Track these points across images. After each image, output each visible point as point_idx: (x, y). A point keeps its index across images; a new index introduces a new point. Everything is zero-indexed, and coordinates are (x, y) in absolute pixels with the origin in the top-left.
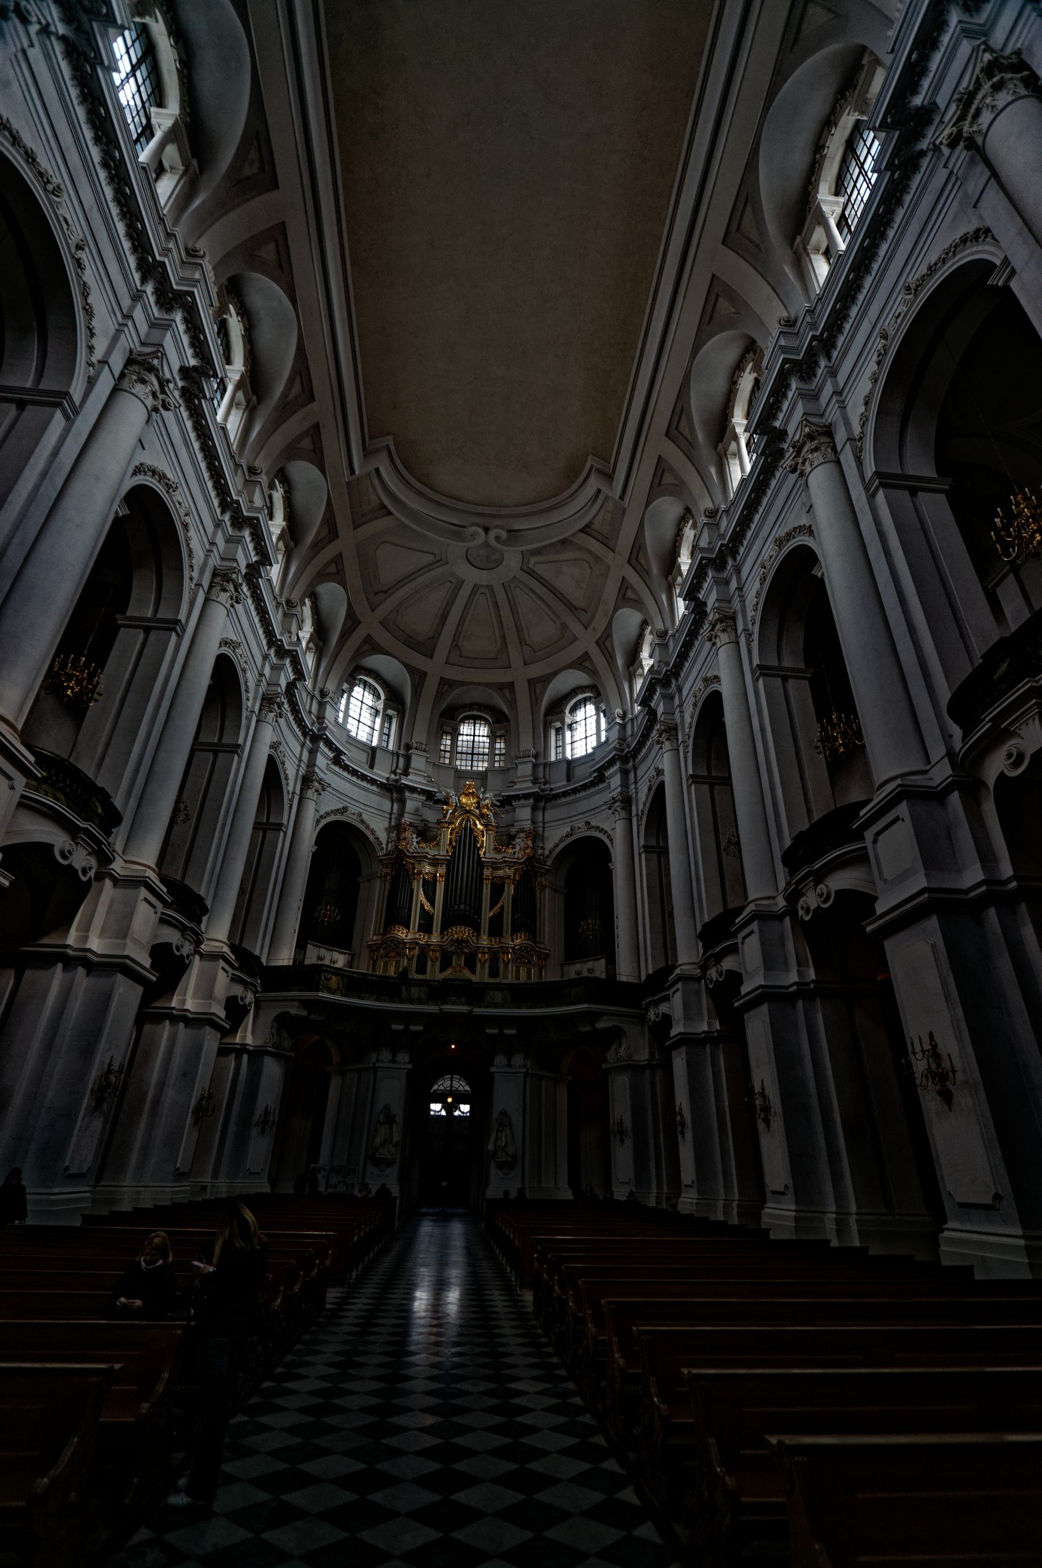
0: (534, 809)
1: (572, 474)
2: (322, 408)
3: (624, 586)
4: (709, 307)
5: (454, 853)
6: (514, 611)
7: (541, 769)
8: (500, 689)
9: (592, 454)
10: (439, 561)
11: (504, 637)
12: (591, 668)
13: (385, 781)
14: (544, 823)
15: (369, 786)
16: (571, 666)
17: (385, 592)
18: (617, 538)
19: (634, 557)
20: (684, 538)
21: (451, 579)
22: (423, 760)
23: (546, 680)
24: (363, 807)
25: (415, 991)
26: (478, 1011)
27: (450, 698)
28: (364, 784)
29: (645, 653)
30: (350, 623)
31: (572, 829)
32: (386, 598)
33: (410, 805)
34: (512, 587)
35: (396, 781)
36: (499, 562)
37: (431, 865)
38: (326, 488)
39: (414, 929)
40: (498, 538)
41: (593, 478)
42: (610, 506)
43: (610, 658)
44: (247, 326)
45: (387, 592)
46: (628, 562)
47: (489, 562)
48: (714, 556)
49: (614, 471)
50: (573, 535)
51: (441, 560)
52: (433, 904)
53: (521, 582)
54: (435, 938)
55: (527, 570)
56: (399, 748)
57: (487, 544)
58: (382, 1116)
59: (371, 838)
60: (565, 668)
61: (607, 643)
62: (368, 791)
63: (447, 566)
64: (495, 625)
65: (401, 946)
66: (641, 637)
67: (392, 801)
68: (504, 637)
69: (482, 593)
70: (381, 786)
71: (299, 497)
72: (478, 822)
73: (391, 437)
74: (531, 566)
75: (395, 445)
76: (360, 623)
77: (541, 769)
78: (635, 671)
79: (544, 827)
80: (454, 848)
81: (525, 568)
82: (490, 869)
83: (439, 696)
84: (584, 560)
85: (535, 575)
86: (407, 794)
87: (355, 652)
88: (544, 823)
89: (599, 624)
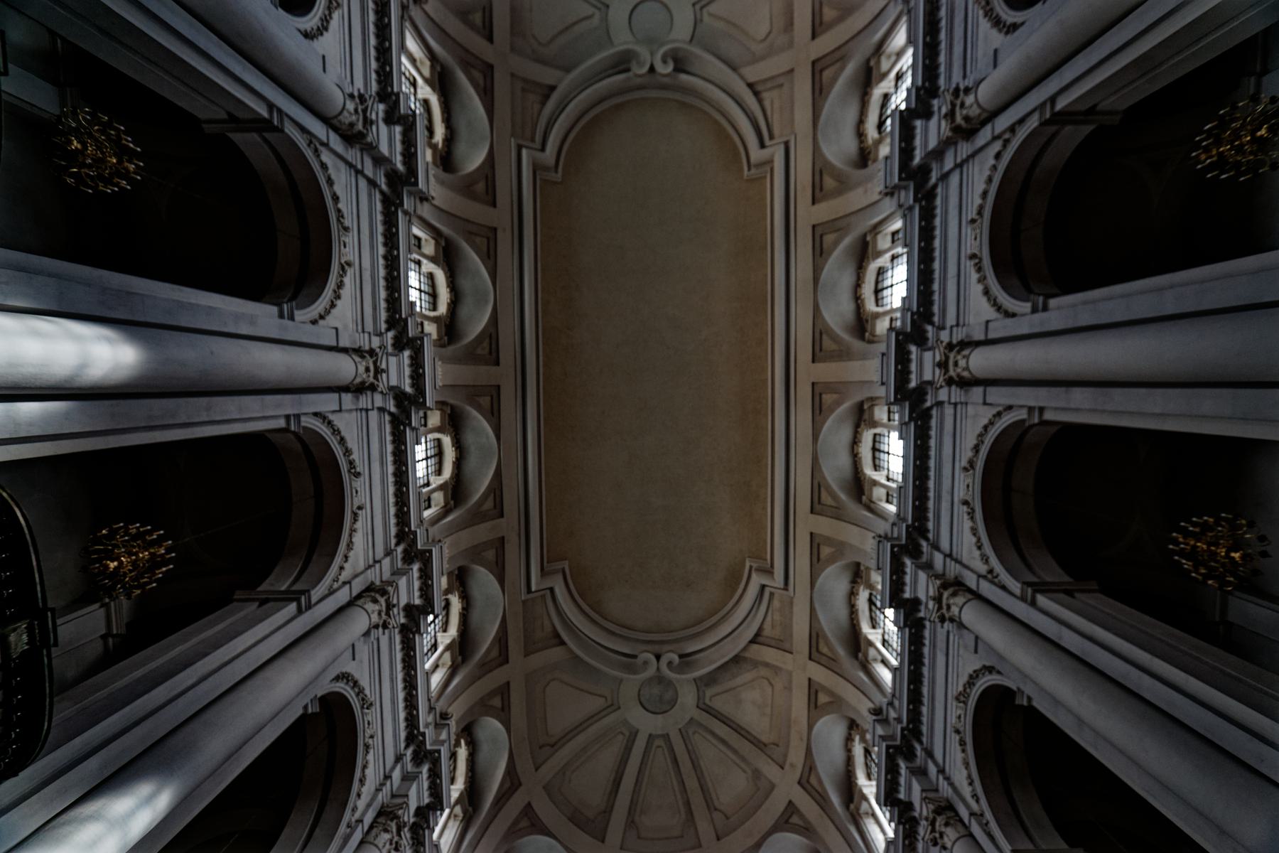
1: (734, 581)
2: (508, 525)
3: (813, 689)
4: (817, 245)
9: (749, 557)
10: (613, 707)
12: (801, 823)
16: (775, 829)
17: (552, 746)
18: (791, 636)
19: (814, 650)
20: (860, 613)
29: (862, 780)
30: (507, 785)
32: (554, 753)
34: (690, 733)
36: (673, 703)
38: (502, 604)
40: (670, 664)
41: (754, 576)
42: (776, 603)
43: (821, 800)
44: (458, 456)
45: (555, 746)
46: (810, 658)
47: (662, 703)
48: (898, 742)
49: (772, 566)
50: (745, 649)
51: (612, 705)
53: (700, 725)
55: (704, 707)
57: (660, 679)
61: (813, 781)
63: (618, 712)
64: (676, 789)
66: (849, 761)
69: (659, 747)
71: (475, 616)
73: (567, 562)
74: (707, 701)
75: (570, 570)
76: (520, 784)
78: (858, 809)
81: (701, 705)
84: (763, 678)
87: (509, 829)
89: (796, 757)
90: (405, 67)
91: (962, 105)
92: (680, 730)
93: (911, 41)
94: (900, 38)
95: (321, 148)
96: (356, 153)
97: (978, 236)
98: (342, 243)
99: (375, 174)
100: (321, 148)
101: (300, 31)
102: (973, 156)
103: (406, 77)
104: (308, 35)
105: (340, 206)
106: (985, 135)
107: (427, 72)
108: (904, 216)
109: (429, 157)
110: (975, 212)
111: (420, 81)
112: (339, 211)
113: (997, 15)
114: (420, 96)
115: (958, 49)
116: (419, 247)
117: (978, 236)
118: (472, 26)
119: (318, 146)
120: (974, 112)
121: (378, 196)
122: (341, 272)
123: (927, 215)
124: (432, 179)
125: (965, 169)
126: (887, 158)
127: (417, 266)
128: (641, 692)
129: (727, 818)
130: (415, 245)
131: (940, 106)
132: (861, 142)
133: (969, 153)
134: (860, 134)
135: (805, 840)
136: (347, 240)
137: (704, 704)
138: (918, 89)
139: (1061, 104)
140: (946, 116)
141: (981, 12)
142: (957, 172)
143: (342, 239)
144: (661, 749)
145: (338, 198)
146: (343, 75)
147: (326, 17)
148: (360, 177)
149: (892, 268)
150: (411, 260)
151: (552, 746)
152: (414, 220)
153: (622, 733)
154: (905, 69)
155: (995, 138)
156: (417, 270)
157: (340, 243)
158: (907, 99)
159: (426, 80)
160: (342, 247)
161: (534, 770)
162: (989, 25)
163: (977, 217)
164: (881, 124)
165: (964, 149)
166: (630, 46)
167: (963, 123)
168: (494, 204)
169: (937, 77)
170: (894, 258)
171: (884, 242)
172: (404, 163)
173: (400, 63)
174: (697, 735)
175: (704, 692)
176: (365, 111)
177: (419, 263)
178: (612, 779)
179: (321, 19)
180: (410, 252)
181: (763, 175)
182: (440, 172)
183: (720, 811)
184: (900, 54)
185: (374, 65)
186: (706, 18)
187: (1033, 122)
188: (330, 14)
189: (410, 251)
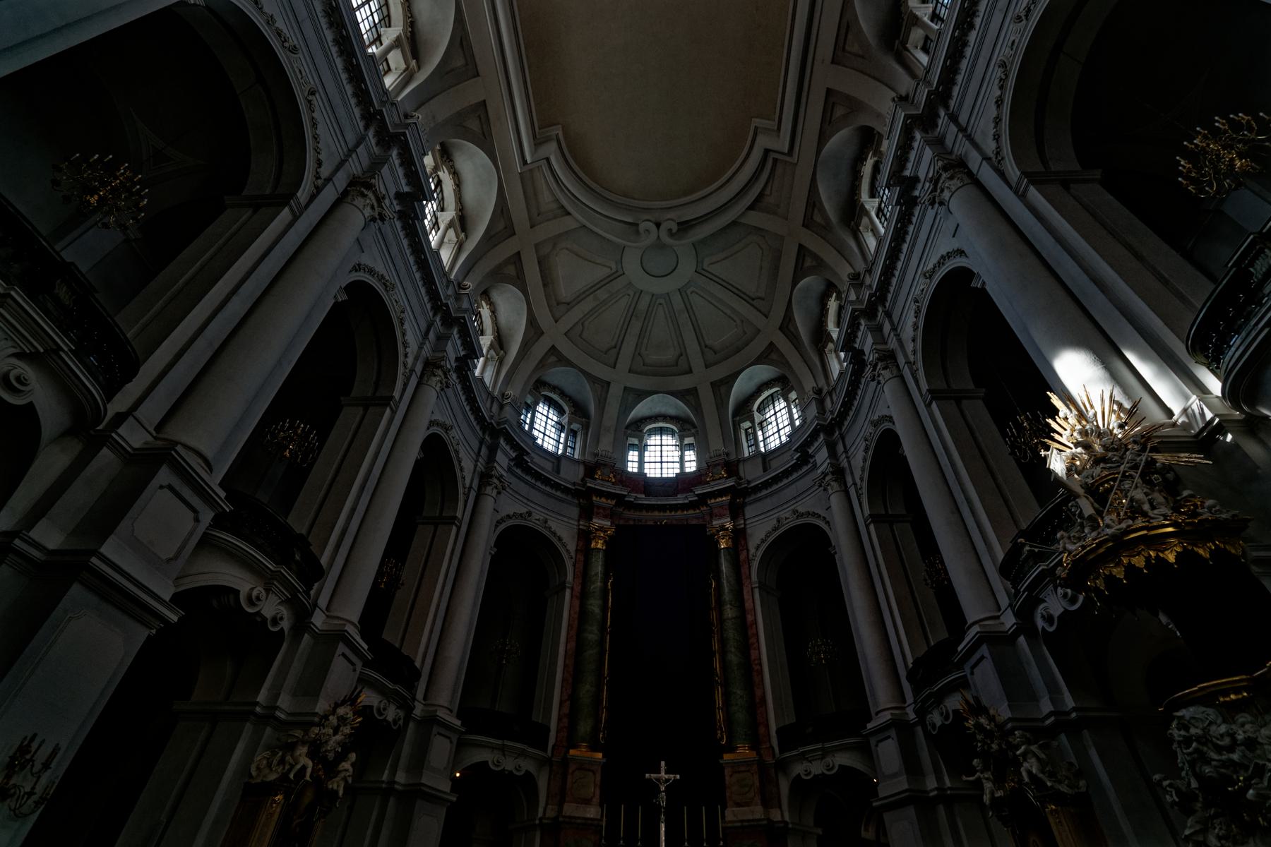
90: (883, 225)
91: (373, 207)
93: (436, 254)
94: (446, 255)
95: (992, 156)
96: (958, 150)
97: (299, 77)
98: (1014, 47)
99: (947, 127)
100: (992, 156)
101: (967, 256)
102: (342, 163)
103: (885, 216)
104: (961, 252)
105: (999, 93)
106: (341, 181)
107: (865, 220)
108: (385, 92)
109: (885, 144)
110: (315, 102)
111: (873, 214)
112: (1001, 88)
113: (373, 276)
114: (877, 200)
115: (394, 251)
116: (927, 38)
117: (299, 77)
118: (816, 257)
119: (994, 159)
120: (359, 202)
121: (952, 103)
122: (1032, 8)
123: (363, 96)
124: (888, 122)
125: (345, 150)
126: (425, 154)
127: (937, 12)
130: (932, 41)
131: (392, 207)
132: (453, 167)
133: (347, 163)
134: (455, 174)
136: (1008, 50)
138: (418, 219)
139: (285, 214)
140: (384, 198)
141: (387, 278)
142: (351, 145)
143: (1013, 52)
145: (997, 102)
146: (942, 220)
147: (939, 266)
148: (963, 123)
149: (375, 25)
150: (942, 20)
152: (921, 73)
154: (433, 232)
155: (329, 180)
156: (939, 5)
157: (1017, 47)
158: (423, 208)
159: (867, 214)
160: (1017, 41)
162: (376, 269)
163: (310, 98)
164: (439, 183)
165: (355, 167)
166: (677, 242)
167: (366, 192)
168: (829, 91)
169: (404, 228)
170: (378, 40)
171: (396, 59)
172: (912, 139)
173: (886, 229)
176: (935, 190)
177: (935, 17)
179: (943, 264)
180: (940, 33)
181: (543, 130)
182: (878, 128)
184: (441, 243)
185: (911, 228)
186: (614, 266)
187: (302, 195)
188: (935, 267)
189: (940, 32)
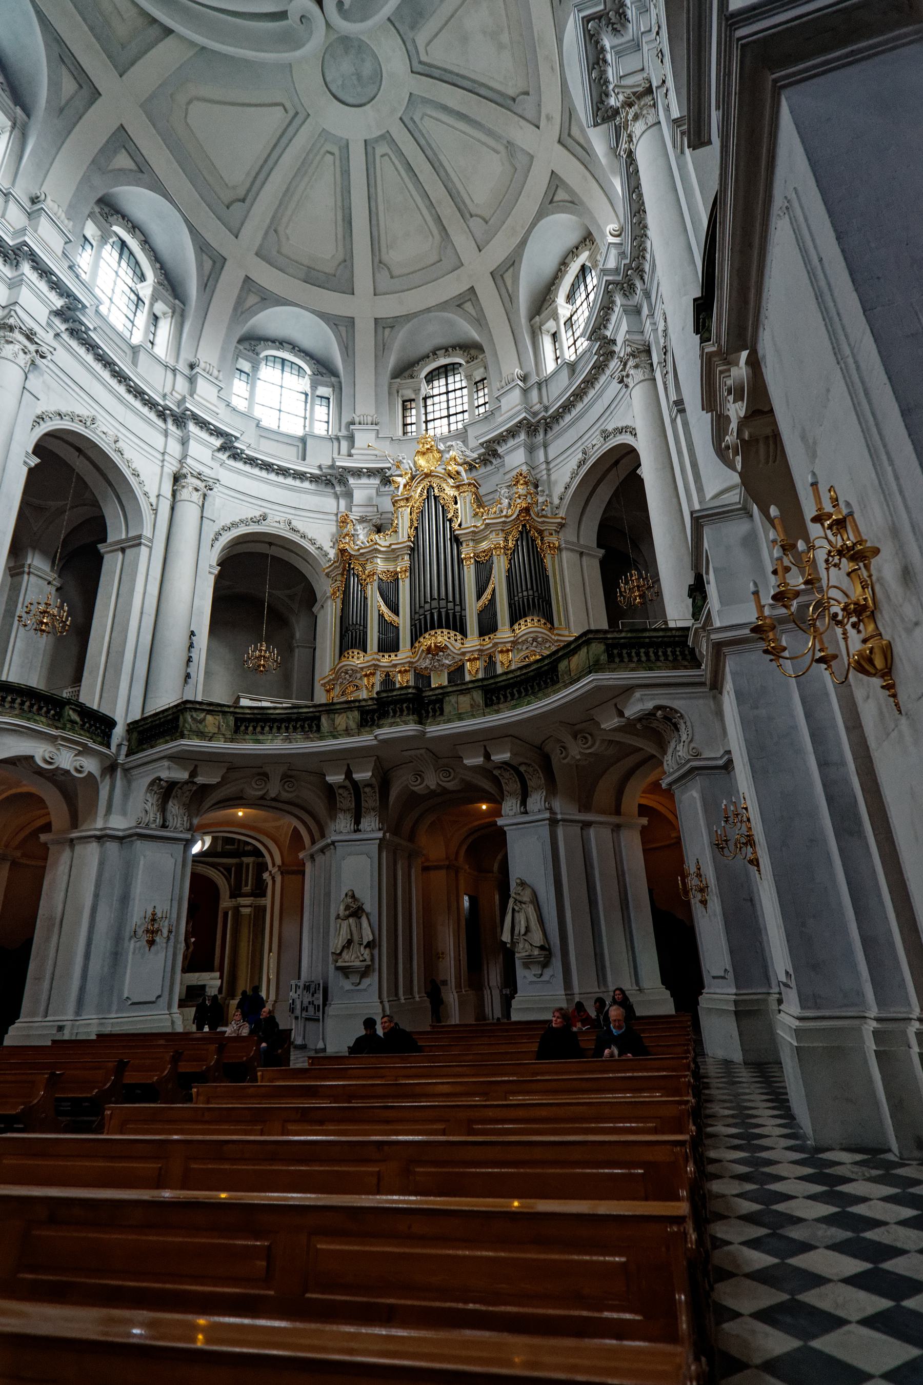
0: (531, 450)
5: (417, 536)
6: (436, 165)
7: (534, 393)
8: (459, 306)
11: (438, 220)
13: (317, 472)
14: (548, 463)
15: (297, 483)
16: (541, 215)
21: (328, 147)
22: (373, 435)
23: (513, 262)
24: (293, 511)
25: (341, 721)
26: (435, 729)
27: (397, 345)
28: (290, 481)
31: (584, 453)
33: (359, 496)
34: (417, 119)
35: (332, 467)
36: (377, 76)
37: (386, 560)
39: (372, 649)
51: (297, 113)
52: (395, 609)
53: (426, 101)
54: (404, 654)
56: (340, 430)
57: (346, 42)
58: (342, 907)
59: (311, 549)
60: (533, 225)
62: (300, 492)
65: (359, 675)
67: (337, 497)
68: (438, 220)
69: (382, 156)
70: (314, 479)
72: (444, 485)
77: (534, 393)
79: (548, 470)
80: (416, 528)
82: (471, 544)
83: (381, 348)
85: (436, 73)
86: (351, 481)
87: (235, 309)
88: (548, 463)
92: (401, 119)
128: (328, 79)
129: (487, 222)
135: (573, 218)
137: (420, 62)
144: (386, 158)
151: (243, 200)
153: (332, 154)
161: (234, 238)
174: (426, 118)
175: (414, 41)
178: (340, 218)
183: (477, 216)
